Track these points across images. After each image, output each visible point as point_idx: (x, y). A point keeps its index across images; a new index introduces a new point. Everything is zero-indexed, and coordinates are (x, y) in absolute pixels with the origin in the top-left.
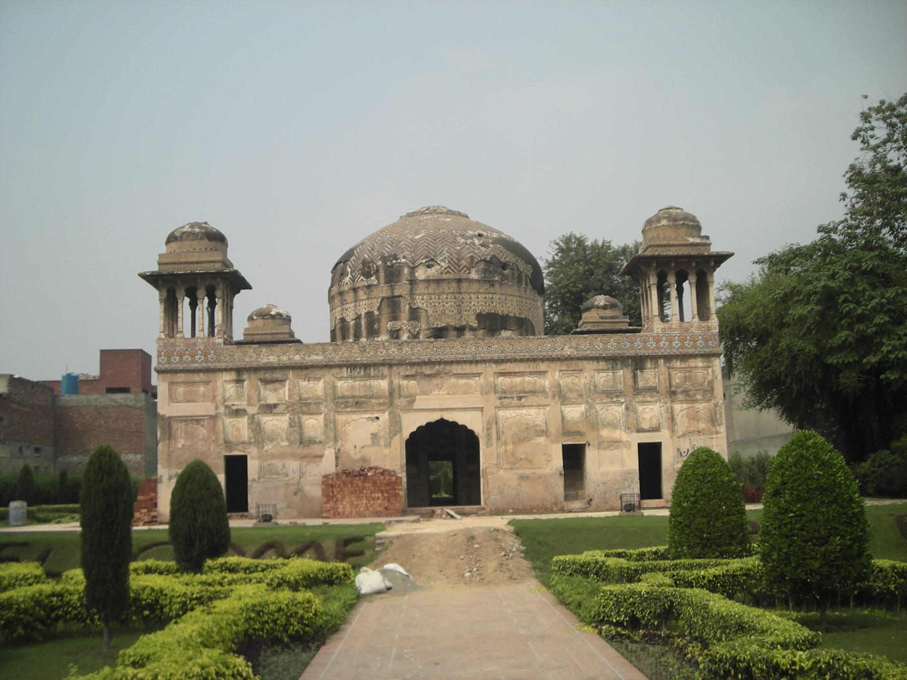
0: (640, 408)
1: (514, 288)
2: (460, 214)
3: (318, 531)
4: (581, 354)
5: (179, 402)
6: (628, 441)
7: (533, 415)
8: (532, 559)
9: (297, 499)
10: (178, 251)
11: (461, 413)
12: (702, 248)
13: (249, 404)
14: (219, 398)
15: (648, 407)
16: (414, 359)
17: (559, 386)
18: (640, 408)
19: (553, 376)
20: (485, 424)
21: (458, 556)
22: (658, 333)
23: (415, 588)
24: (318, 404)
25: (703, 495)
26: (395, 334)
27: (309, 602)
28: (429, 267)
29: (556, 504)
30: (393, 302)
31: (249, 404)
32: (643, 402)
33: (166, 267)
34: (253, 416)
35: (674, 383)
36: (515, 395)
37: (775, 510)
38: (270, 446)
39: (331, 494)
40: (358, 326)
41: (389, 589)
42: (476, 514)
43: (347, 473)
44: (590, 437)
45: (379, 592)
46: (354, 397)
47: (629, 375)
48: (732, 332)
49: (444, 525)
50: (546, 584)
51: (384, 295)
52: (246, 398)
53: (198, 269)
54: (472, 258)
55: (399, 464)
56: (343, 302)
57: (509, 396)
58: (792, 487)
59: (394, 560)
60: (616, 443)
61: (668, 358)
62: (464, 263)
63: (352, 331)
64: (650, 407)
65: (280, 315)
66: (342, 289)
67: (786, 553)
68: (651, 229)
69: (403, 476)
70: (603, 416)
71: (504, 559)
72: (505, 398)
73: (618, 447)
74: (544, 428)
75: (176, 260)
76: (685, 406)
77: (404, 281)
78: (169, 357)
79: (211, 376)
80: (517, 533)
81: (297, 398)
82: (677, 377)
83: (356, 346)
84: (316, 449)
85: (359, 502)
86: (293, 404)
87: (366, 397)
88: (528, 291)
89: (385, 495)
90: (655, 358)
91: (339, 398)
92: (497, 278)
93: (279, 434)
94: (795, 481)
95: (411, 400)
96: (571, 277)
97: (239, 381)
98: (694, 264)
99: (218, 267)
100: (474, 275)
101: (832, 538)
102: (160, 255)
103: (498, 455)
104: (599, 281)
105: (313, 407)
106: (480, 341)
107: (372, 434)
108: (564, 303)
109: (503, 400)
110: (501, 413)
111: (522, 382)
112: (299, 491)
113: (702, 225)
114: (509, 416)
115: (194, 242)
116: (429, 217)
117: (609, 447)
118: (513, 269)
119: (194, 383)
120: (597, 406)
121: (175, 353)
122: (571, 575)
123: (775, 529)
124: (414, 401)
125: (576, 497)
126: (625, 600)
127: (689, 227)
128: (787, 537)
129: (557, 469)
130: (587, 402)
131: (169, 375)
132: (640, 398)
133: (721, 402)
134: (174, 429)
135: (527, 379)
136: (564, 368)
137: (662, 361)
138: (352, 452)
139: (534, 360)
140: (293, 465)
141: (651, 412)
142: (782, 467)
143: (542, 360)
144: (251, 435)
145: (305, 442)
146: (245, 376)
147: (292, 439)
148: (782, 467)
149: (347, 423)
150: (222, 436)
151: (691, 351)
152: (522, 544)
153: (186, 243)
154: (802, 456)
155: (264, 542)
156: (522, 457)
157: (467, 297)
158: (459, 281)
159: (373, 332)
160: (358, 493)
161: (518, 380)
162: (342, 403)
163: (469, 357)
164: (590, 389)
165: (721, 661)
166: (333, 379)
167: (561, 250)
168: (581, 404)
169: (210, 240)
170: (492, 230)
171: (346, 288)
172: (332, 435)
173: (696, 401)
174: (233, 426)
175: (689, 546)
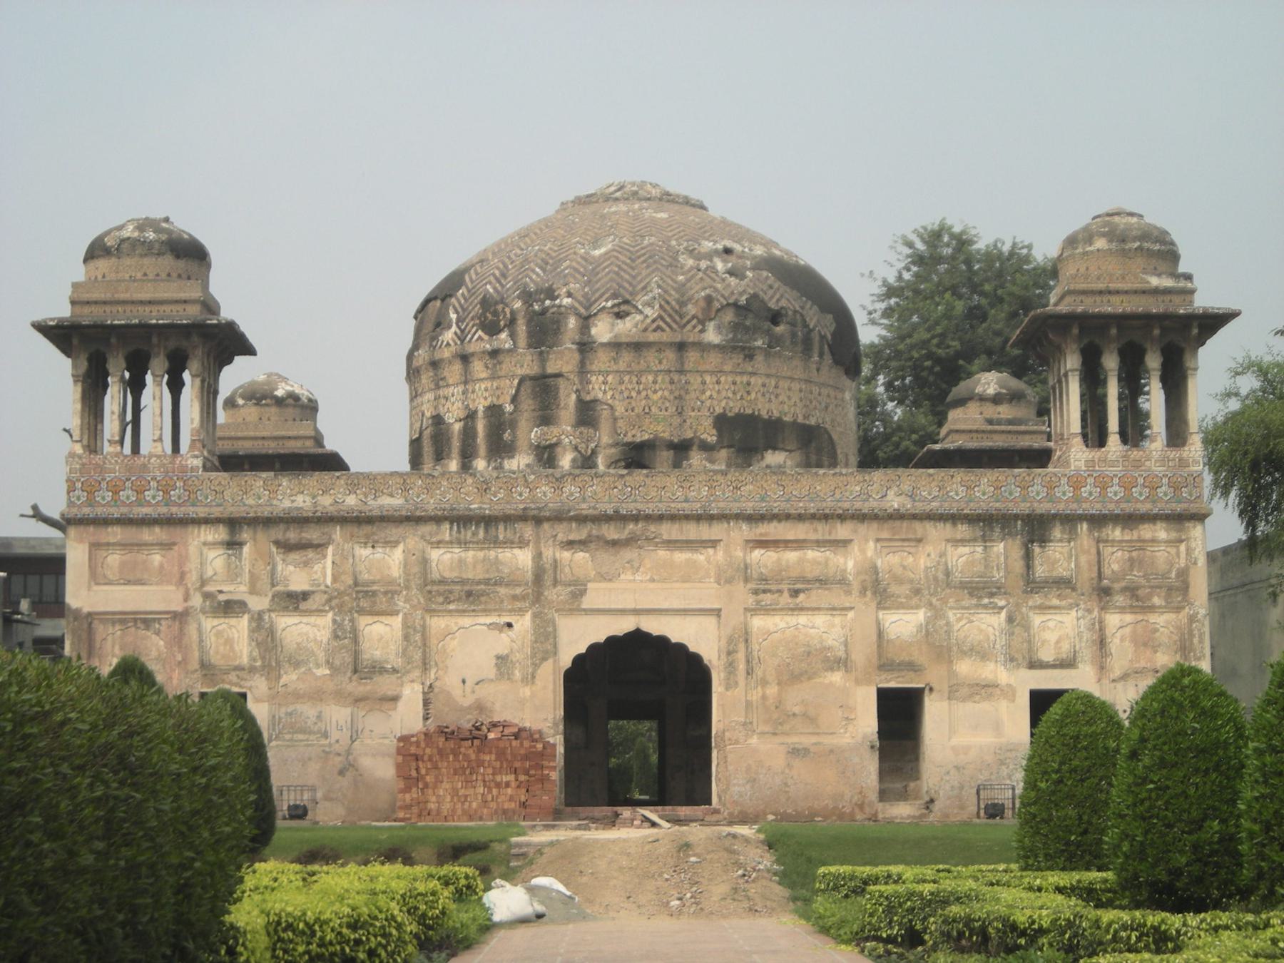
0: (1037, 620)
1: (796, 362)
2: (687, 202)
3: (402, 833)
4: (920, 507)
5: (110, 583)
6: (1009, 686)
7: (821, 627)
8: (792, 886)
9: (345, 782)
10: (112, 276)
12: (1177, 299)
13: (253, 591)
14: (192, 578)
15: (1053, 619)
16: (585, 508)
17: (875, 569)
18: (1037, 620)
19: (863, 551)
20: (724, 642)
21: (661, 875)
23: (585, 917)
24: (391, 594)
25: (1073, 770)
26: (546, 455)
27: (434, 893)
28: (620, 316)
29: (861, 807)
30: (543, 388)
31: (253, 591)
32: (1043, 608)
33: (86, 310)
34: (260, 615)
35: (1107, 572)
36: (785, 587)
37: (1130, 779)
38: (294, 677)
39: (414, 773)
40: (468, 434)
41: (540, 916)
42: (701, 821)
43: (447, 733)
44: (932, 675)
45: (524, 921)
46: (463, 582)
47: (1017, 552)
48: (1255, 466)
49: (634, 835)
50: (805, 915)
51: (528, 372)
52: (247, 577)
53: (155, 317)
54: (709, 300)
55: (551, 717)
56: (438, 383)
57: (773, 587)
58: (1155, 747)
59: (545, 875)
60: (985, 689)
61: (1098, 521)
62: (691, 309)
63: (456, 444)
64: (1058, 618)
65: (294, 397)
66: (437, 356)
67: (1142, 843)
68: (1072, 256)
69: (558, 741)
70: (961, 634)
71: (741, 881)
72: (764, 591)
73: (989, 697)
74: (841, 654)
75: (108, 296)
76: (1129, 618)
77: (568, 343)
79: (178, 532)
80: (770, 845)
81: (351, 582)
82: (1115, 560)
83: (470, 481)
84: (384, 684)
85: (471, 791)
86: (341, 594)
87: (487, 582)
88: (825, 369)
89: (522, 778)
91: (433, 582)
92: (759, 343)
93: (313, 653)
94: (1159, 737)
95: (579, 591)
96: (937, 323)
97: (233, 545)
98: (1157, 332)
100: (712, 335)
101: (1208, 822)
102: (76, 286)
103: (748, 704)
104: (998, 333)
105: (382, 602)
106: (719, 477)
107: (498, 657)
108: (920, 382)
109: (761, 596)
110: (758, 622)
111: (801, 561)
112: (348, 767)
113: (1182, 250)
115: (146, 261)
116: (622, 207)
117: (970, 697)
118: (793, 324)
119: (141, 545)
120: (950, 614)
121: (104, 485)
122: (847, 896)
123: (1128, 808)
124: (583, 592)
125: (903, 796)
126: (900, 905)
127: (1151, 254)
128: (1144, 819)
129: (865, 737)
130: (931, 604)
131: (91, 529)
132: (1037, 599)
133: (1203, 612)
134: (98, 638)
135: (811, 554)
136: (885, 535)
137: (1085, 526)
138: (457, 692)
139: (826, 517)
140: (338, 714)
141: (1059, 627)
142: (1144, 716)
143: (842, 518)
144: (256, 653)
145: (361, 668)
146: (245, 535)
147: (337, 662)
148: (1144, 716)
149: (449, 633)
150: (196, 654)
151: (1144, 508)
152: (778, 861)
153: (128, 261)
154: (1173, 700)
155: (305, 848)
156: (796, 710)
157: (695, 381)
158: (681, 347)
159: (500, 448)
160: (467, 772)
161: (791, 556)
162: (439, 594)
163: (696, 507)
164: (936, 579)
165: (954, 921)
166: (422, 544)
167: (919, 259)
168: (918, 607)
169: (178, 257)
170: (754, 238)
171: (447, 354)
172: (417, 656)
173: (1152, 609)
174: (219, 634)
175: (1046, 855)
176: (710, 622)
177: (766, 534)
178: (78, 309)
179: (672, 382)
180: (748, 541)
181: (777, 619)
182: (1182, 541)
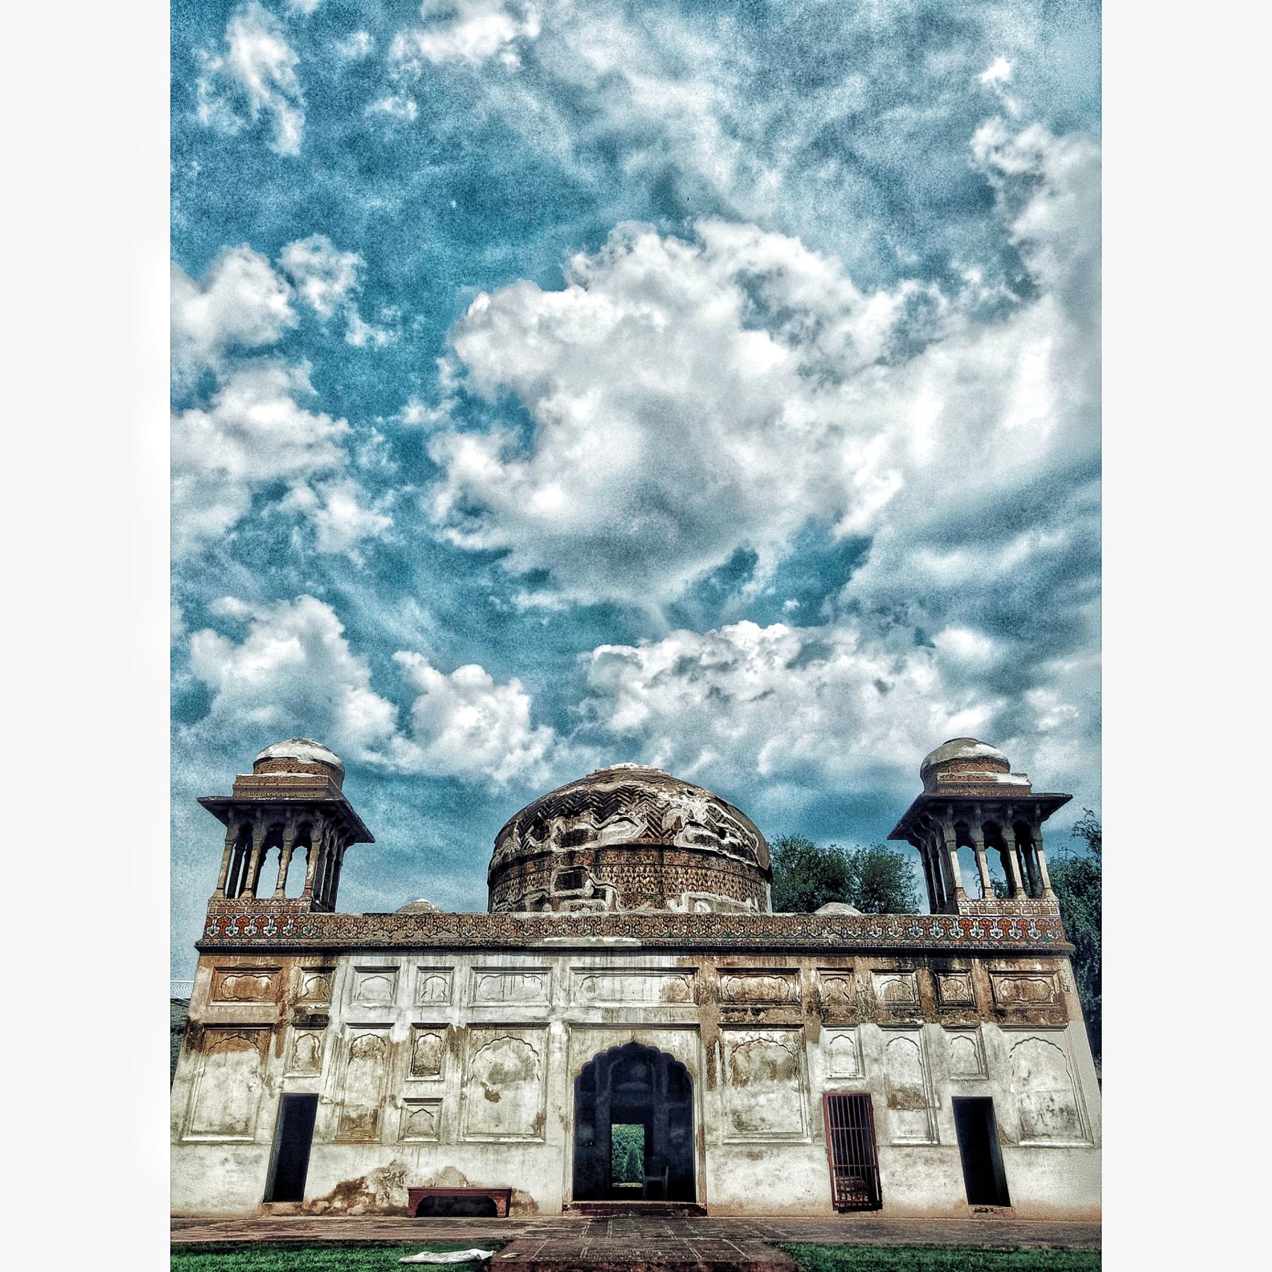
11: (663, 1034)
17: (816, 993)
19: (808, 978)
22: (965, 915)
35: (1000, 998)
61: (987, 955)
72: (733, 1010)
78: (223, 928)
82: (1004, 988)
90: (966, 954)
98: (1010, 812)
99: (320, 796)
111: (761, 985)
114: (740, 1042)
135: (767, 980)
161: (752, 982)
176: (690, 1036)
177: (732, 964)
178: (238, 794)
179: (656, 871)
180: (718, 969)
181: (743, 1033)
182: (1053, 972)
